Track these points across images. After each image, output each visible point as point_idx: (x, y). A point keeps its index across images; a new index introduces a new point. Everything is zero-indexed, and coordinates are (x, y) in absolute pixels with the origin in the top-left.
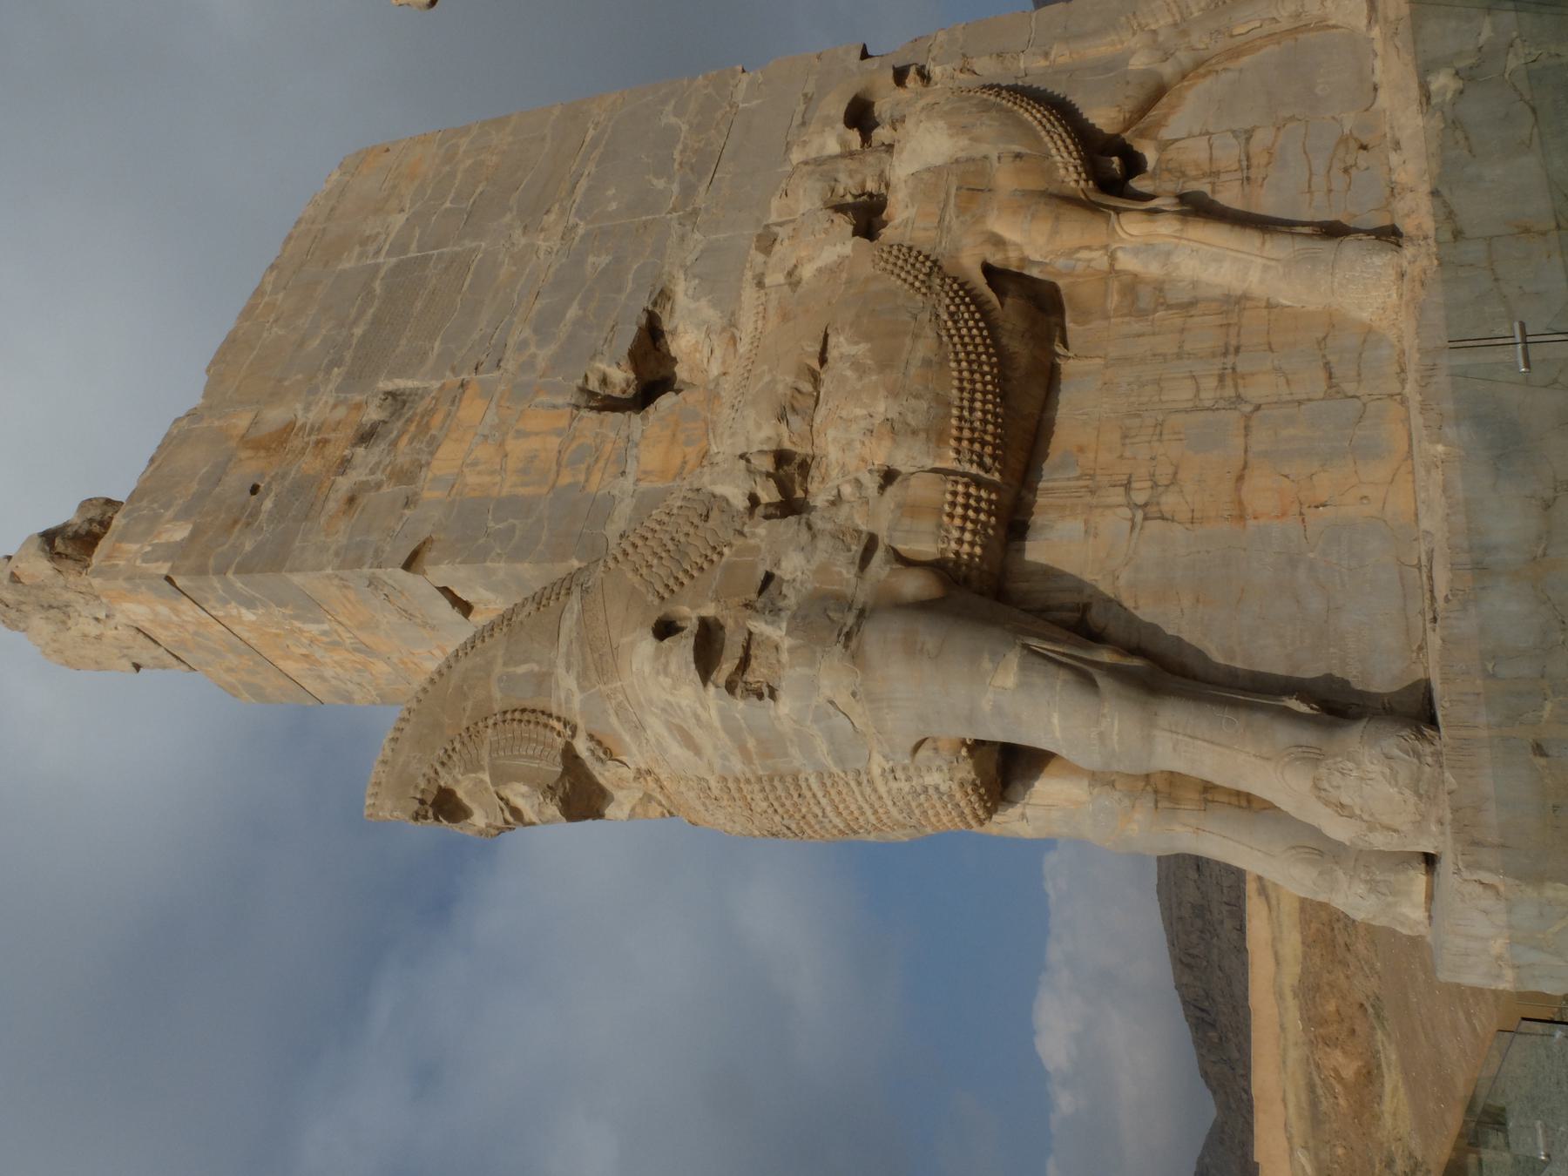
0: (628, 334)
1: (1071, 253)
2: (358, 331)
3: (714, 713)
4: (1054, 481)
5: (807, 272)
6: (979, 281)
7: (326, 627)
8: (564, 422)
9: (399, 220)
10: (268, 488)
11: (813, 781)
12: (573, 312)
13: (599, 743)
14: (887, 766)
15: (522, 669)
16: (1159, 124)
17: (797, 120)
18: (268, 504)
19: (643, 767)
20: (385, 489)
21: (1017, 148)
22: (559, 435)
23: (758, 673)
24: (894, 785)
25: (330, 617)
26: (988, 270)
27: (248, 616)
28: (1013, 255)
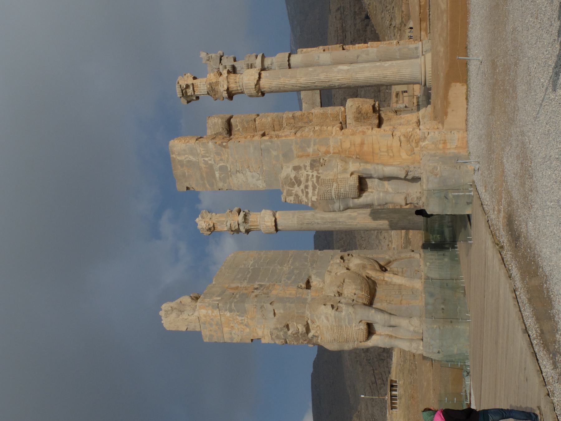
0: (305, 281)
1: (378, 276)
2: (248, 276)
3: (333, 314)
4: (376, 300)
5: (338, 274)
6: (366, 278)
7: (243, 318)
8: (296, 290)
9: (251, 263)
10: (237, 294)
11: (344, 328)
12: (293, 277)
13: (312, 321)
14: (355, 325)
15: (300, 311)
16: (390, 266)
17: (330, 258)
18: (237, 296)
19: (318, 325)
20: (263, 295)
21: (370, 263)
22: (295, 291)
23: (339, 310)
24: (356, 328)
25: (246, 316)
26: (366, 276)
27: (228, 314)
28: (370, 275)
